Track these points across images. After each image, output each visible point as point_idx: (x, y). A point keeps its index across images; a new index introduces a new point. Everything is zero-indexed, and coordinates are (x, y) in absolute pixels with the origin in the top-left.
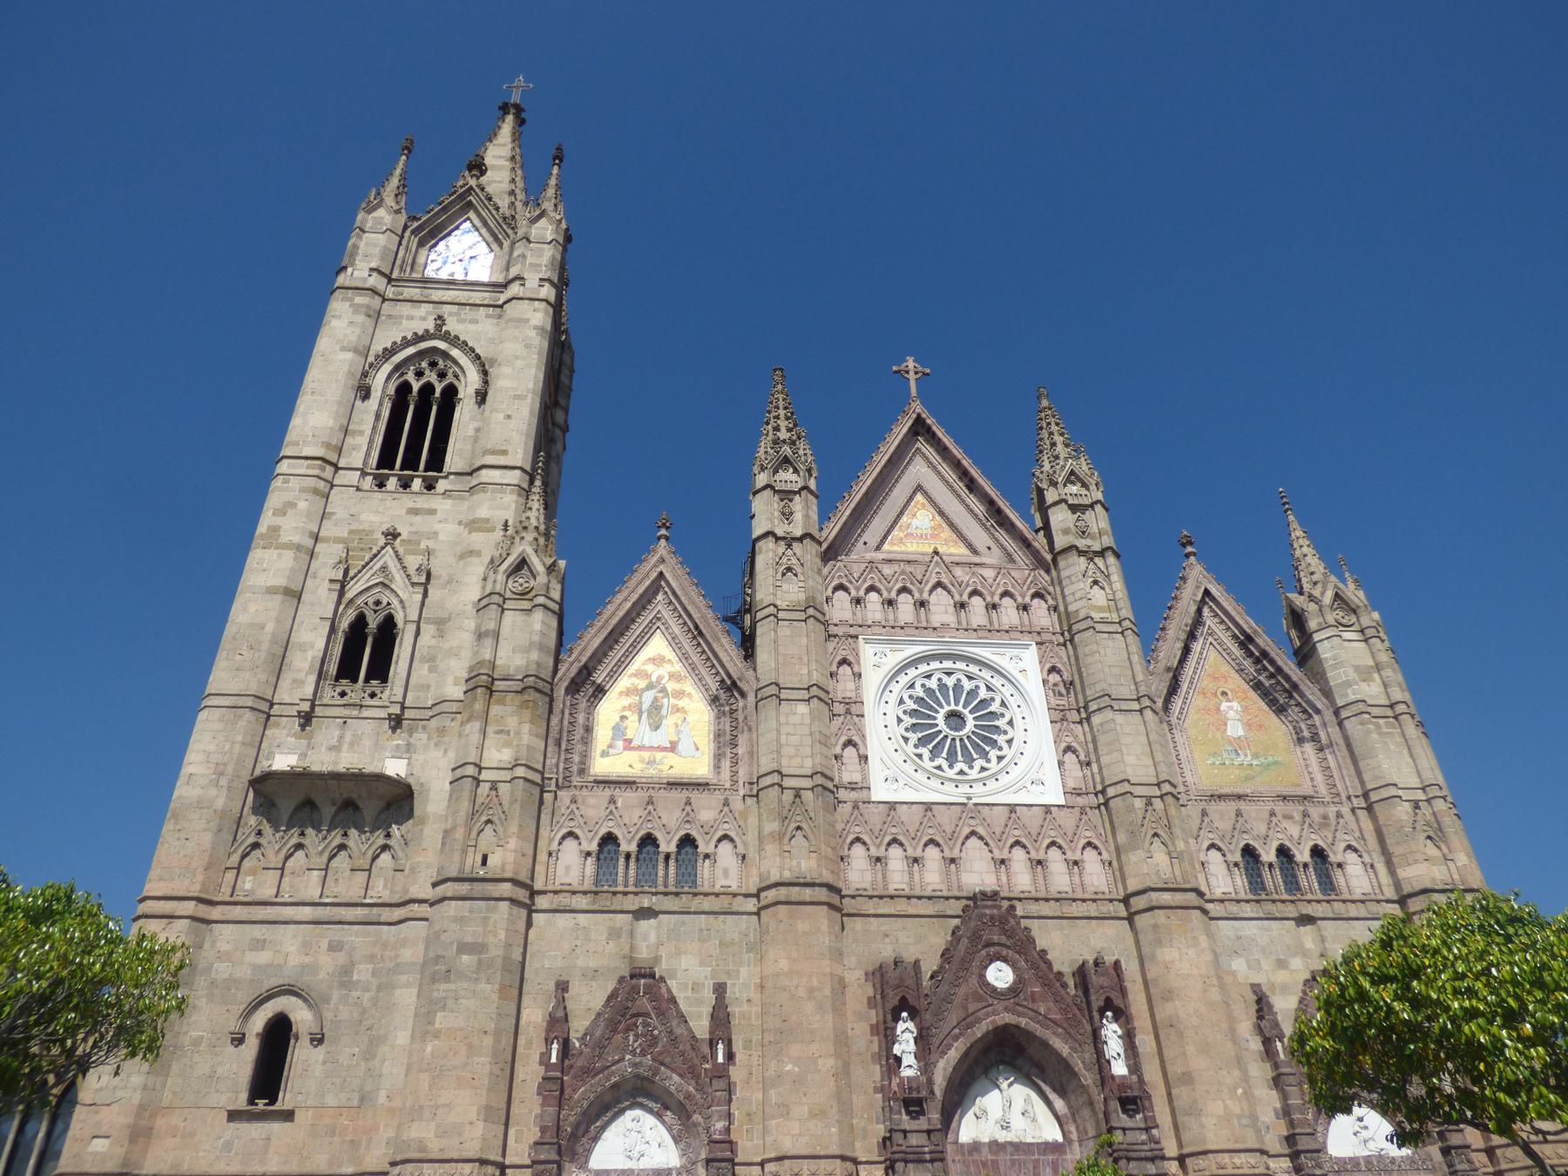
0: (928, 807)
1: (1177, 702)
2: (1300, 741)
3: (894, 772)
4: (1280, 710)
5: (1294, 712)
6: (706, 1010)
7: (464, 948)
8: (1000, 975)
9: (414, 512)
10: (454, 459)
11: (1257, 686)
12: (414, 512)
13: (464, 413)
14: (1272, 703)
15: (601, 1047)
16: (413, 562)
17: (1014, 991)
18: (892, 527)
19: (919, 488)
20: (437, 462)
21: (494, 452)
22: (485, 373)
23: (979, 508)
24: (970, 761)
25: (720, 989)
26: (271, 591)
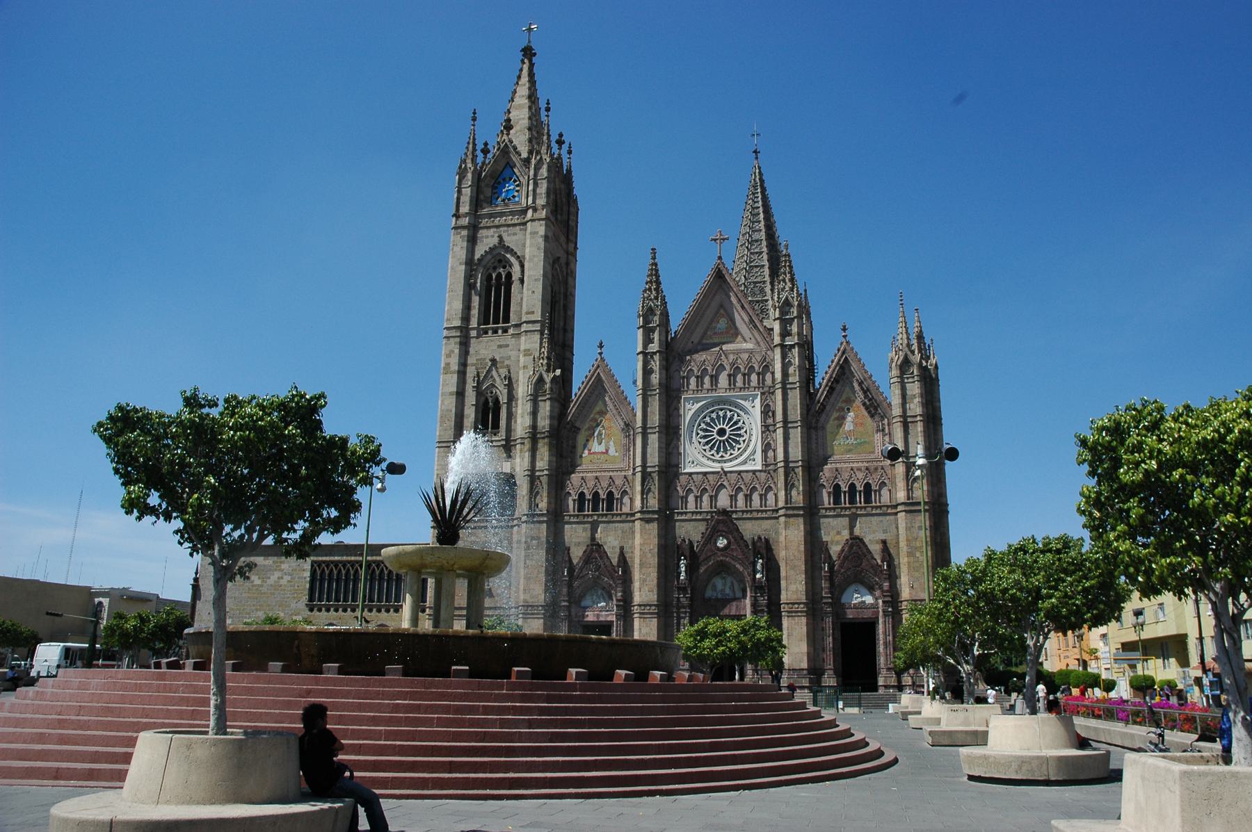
0: (705, 474)
1: (824, 416)
2: (878, 431)
3: (696, 459)
4: (872, 416)
5: (877, 418)
6: (617, 556)
7: (533, 538)
8: (721, 543)
9: (500, 346)
10: (514, 319)
11: (864, 404)
12: (500, 346)
13: (515, 287)
14: (869, 412)
15: (581, 569)
16: (503, 372)
17: (726, 548)
18: (706, 331)
19: (721, 306)
20: (507, 319)
21: (528, 313)
22: (522, 266)
23: (746, 319)
24: (726, 451)
25: (622, 548)
26: (451, 394)
